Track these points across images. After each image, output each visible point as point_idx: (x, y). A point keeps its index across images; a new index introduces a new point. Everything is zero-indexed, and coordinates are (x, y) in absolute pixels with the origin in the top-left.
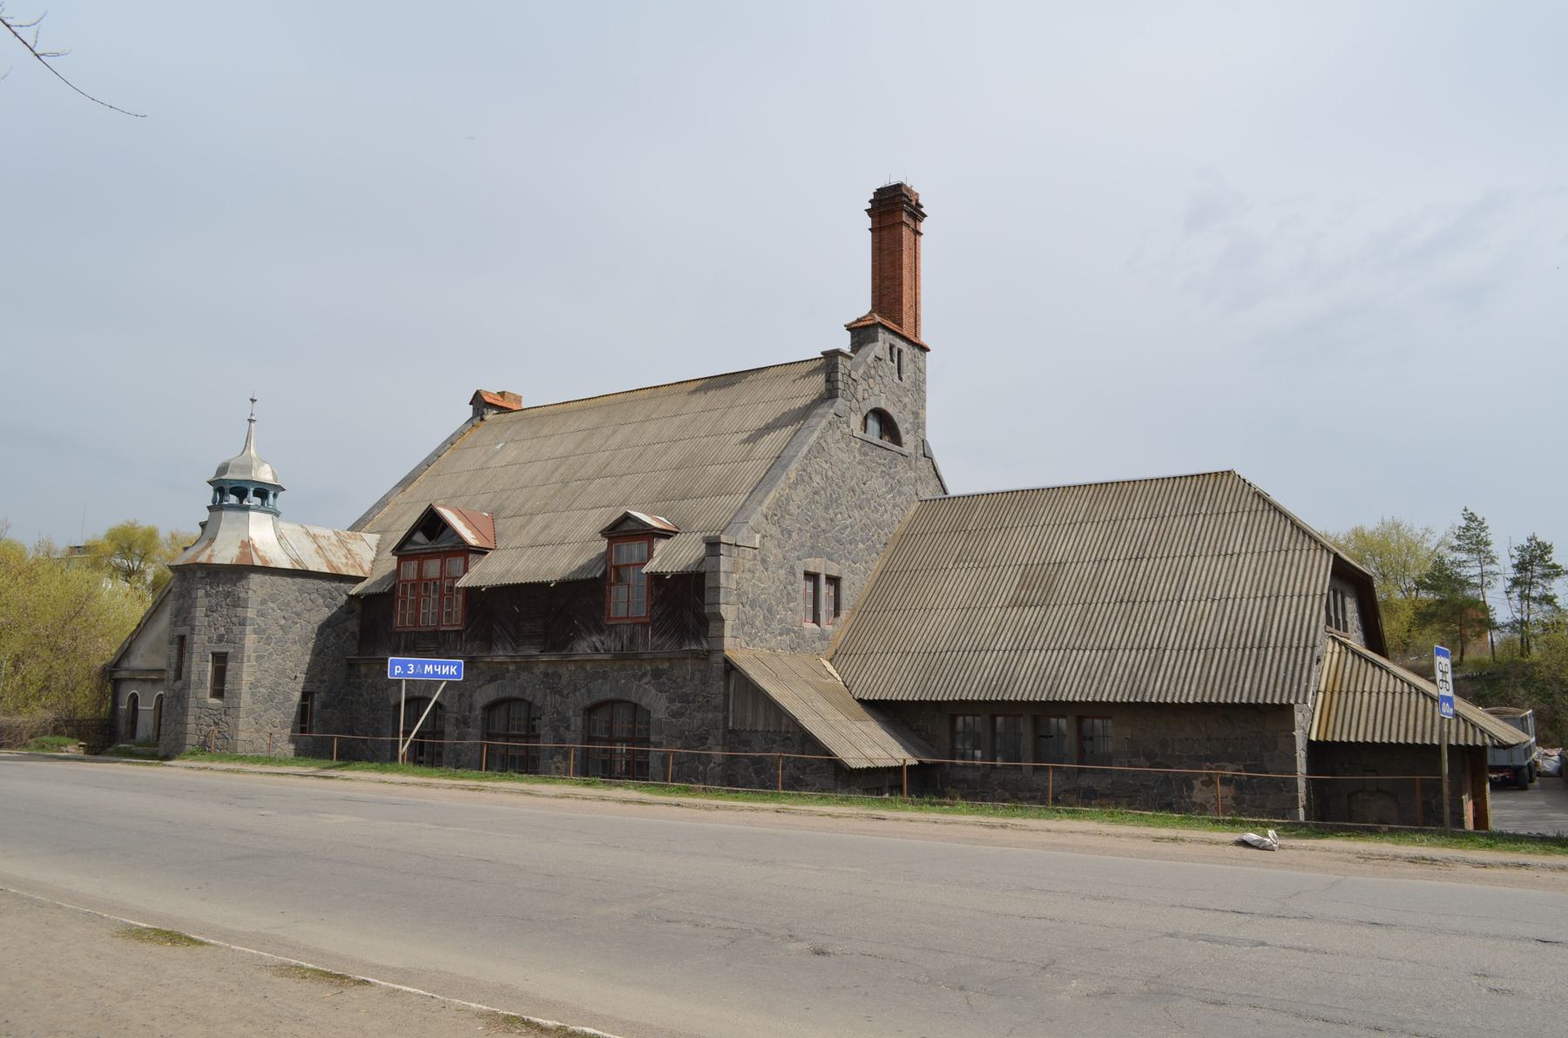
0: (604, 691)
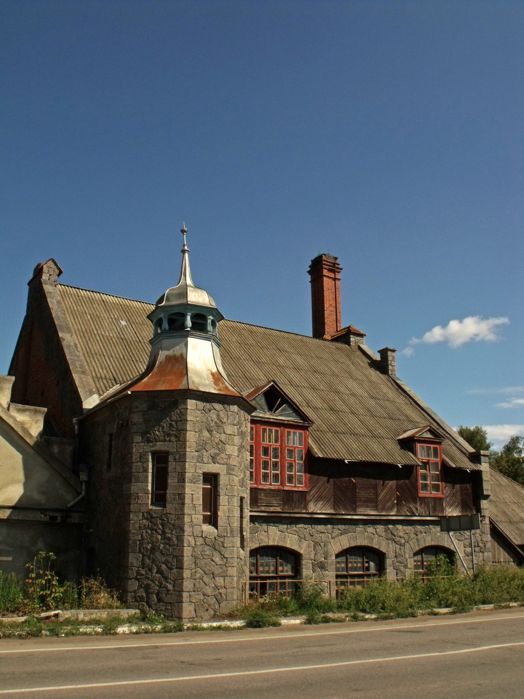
0: (429, 541)
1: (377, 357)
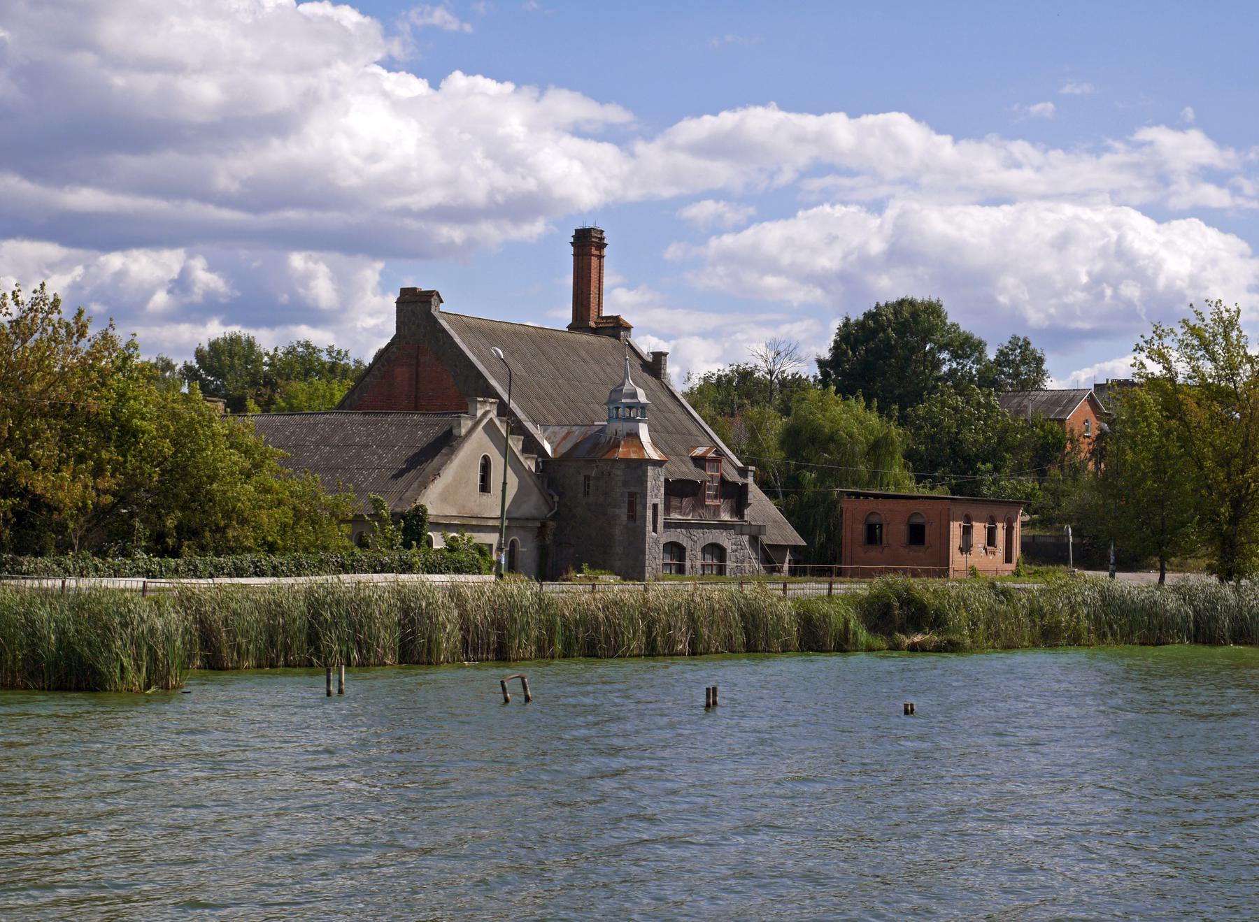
1: (650, 359)
